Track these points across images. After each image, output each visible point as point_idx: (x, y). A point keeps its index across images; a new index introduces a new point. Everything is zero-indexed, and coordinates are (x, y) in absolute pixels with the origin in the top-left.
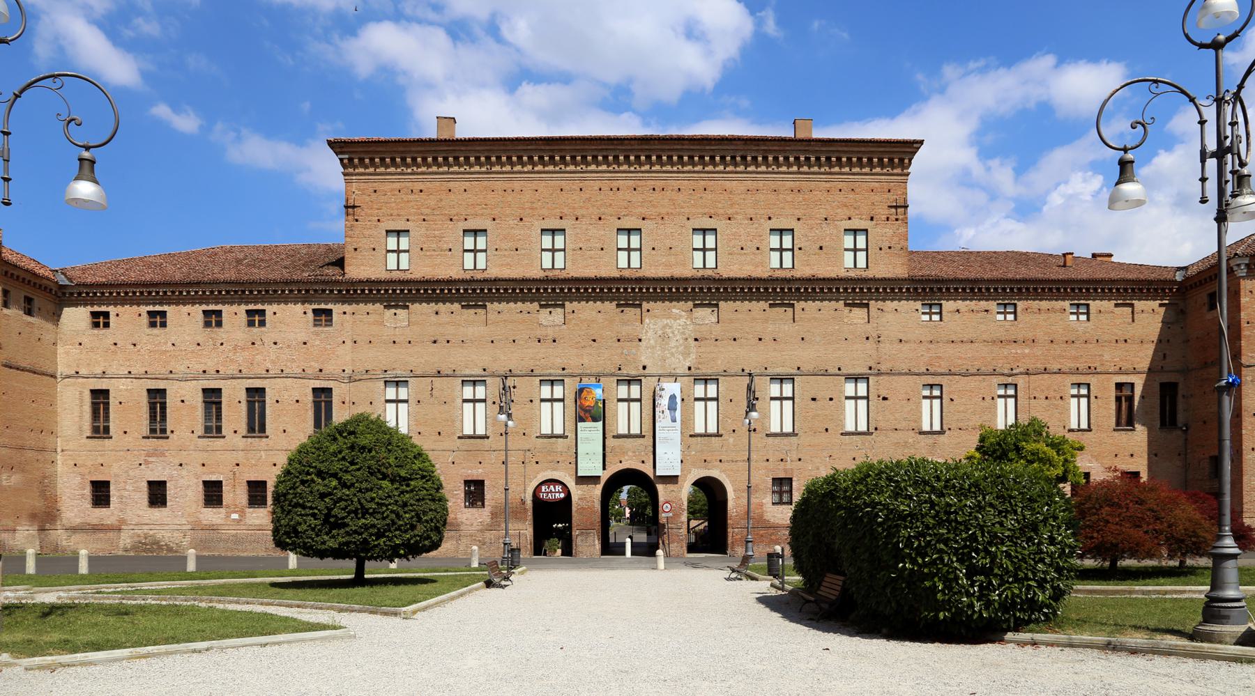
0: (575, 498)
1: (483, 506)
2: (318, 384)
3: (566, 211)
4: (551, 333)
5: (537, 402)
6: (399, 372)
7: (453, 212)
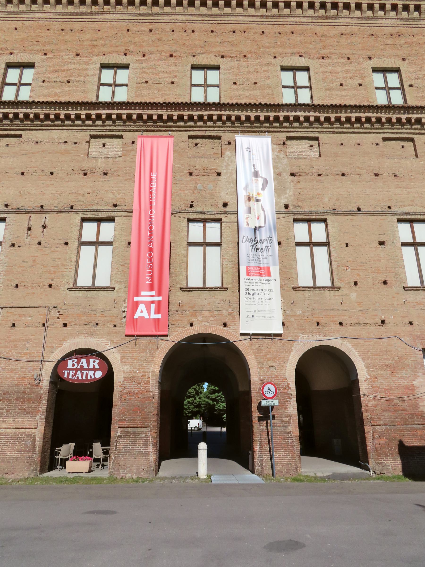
0: (118, 378)
3: (131, 48)
4: (101, 165)
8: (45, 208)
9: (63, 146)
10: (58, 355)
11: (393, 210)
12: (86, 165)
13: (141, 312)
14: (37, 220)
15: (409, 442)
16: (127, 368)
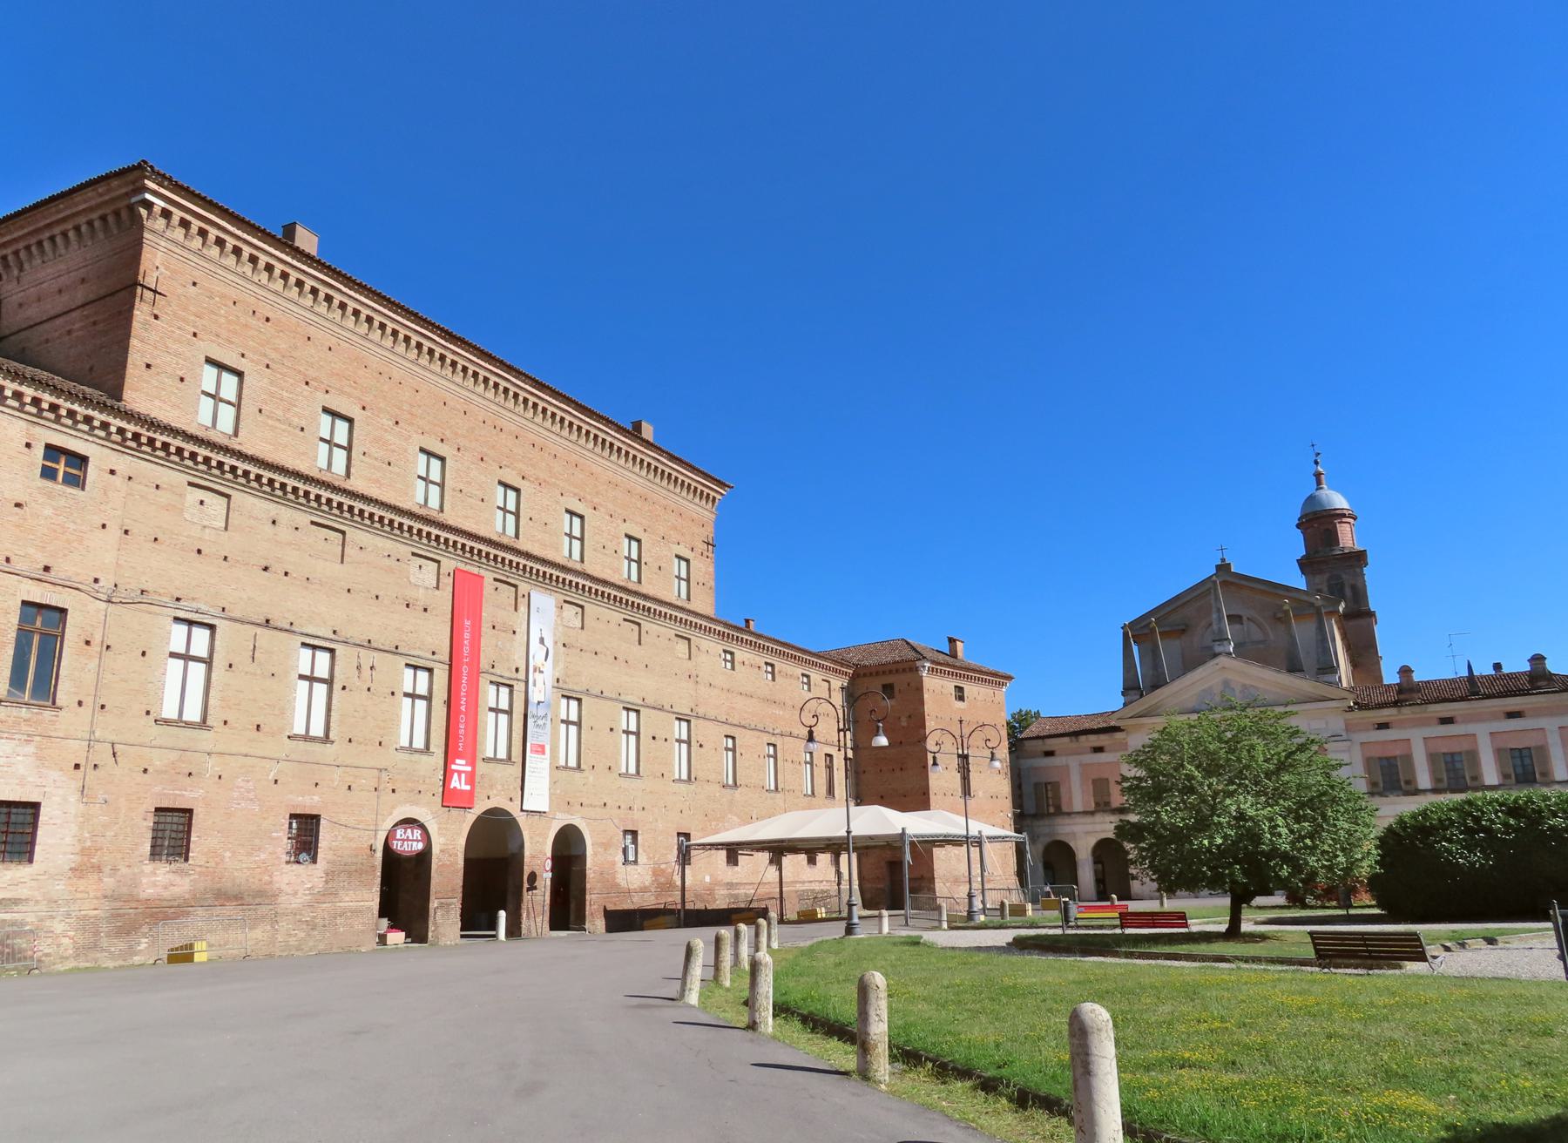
0: (435, 850)
1: (314, 861)
2: (39, 594)
4: (421, 596)
5: (399, 695)
6: (204, 608)
7: (312, 373)
8: (374, 644)
9: (387, 561)
10: (389, 824)
11: (622, 698)
12: (411, 594)
13: (455, 783)
14: (367, 657)
15: (610, 907)
16: (442, 840)
